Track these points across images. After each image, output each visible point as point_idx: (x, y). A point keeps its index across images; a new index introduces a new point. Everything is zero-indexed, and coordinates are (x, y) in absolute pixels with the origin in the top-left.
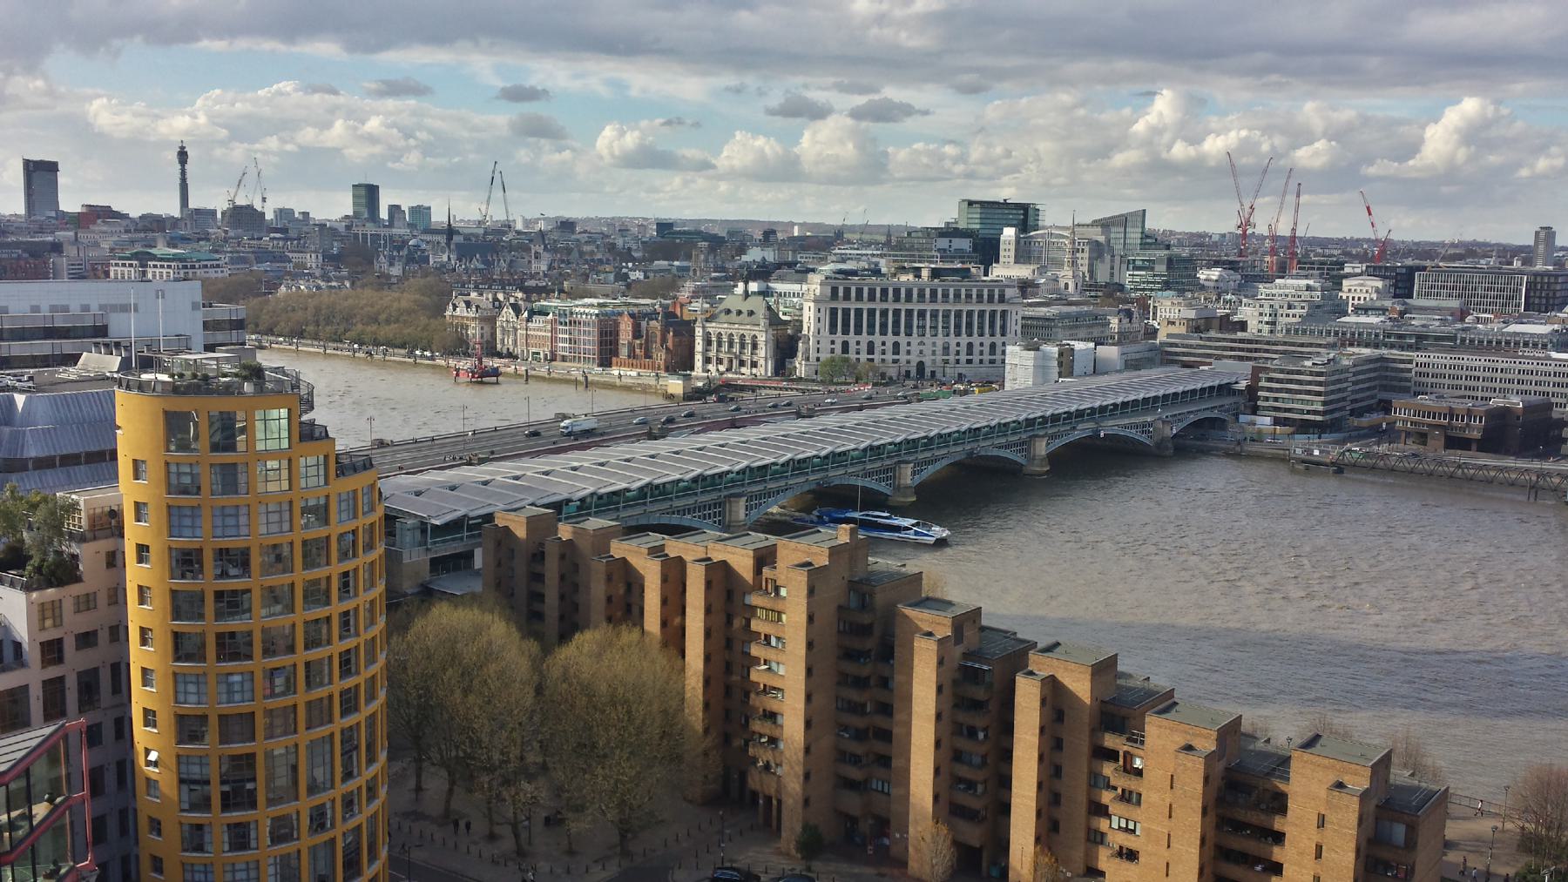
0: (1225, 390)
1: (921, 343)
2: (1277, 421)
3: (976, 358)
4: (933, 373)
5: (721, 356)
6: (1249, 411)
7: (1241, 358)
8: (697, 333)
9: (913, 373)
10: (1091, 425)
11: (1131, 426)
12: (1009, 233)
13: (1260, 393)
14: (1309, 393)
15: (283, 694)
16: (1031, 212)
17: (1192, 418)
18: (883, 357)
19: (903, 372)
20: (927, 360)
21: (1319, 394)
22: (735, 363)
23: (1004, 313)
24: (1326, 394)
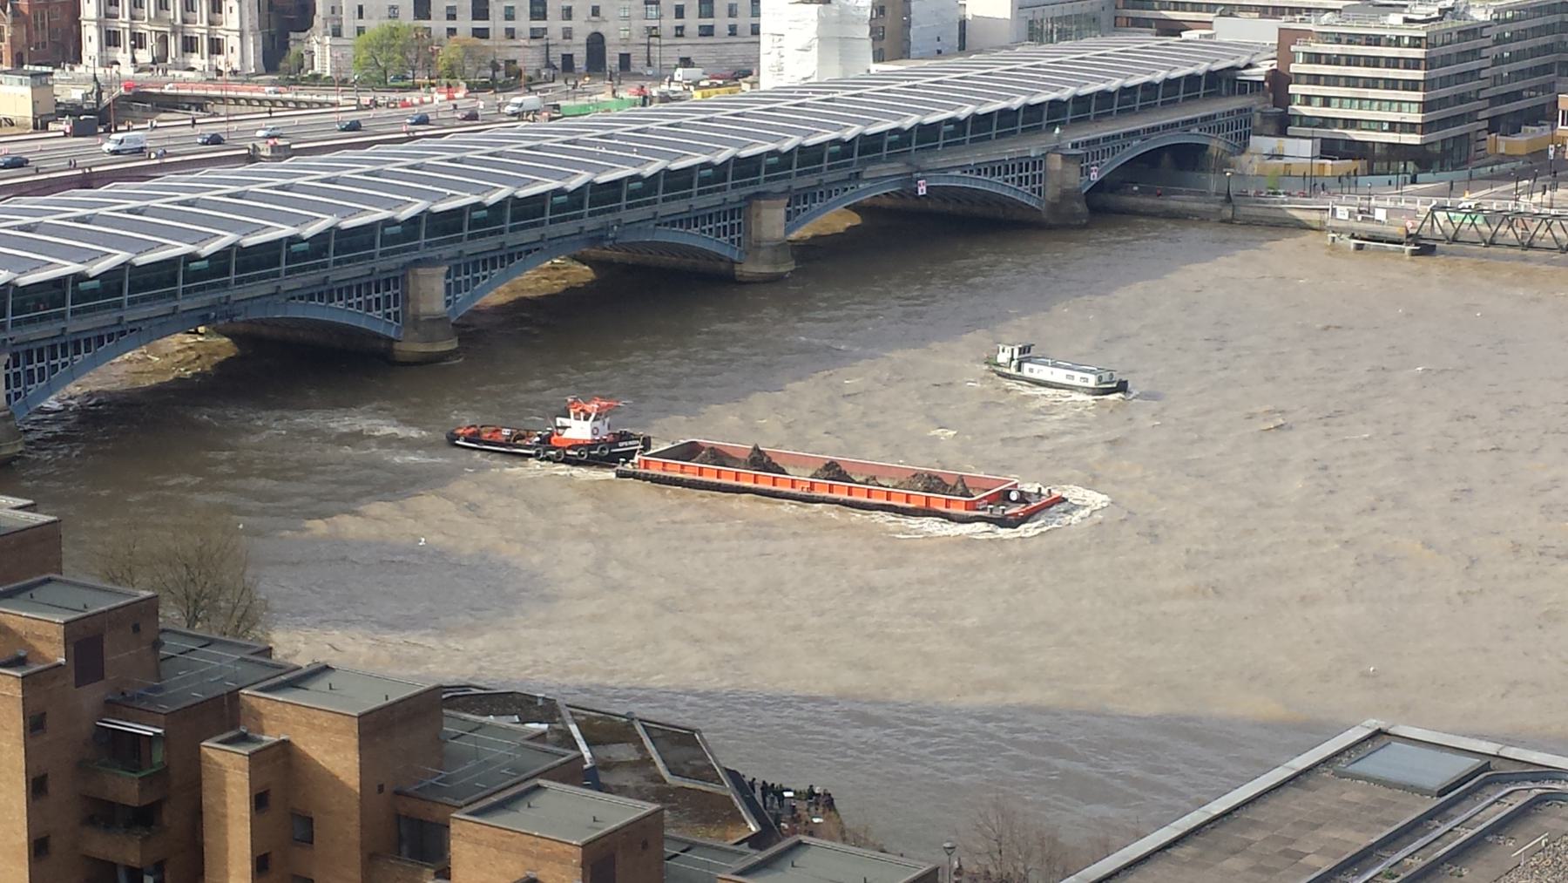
0: (1222, 82)
4: (625, 60)
5: (143, 27)
6: (1271, 127)
10: (897, 167)
11: (993, 169)
13: (1293, 89)
14: (1392, 84)
17: (1138, 147)
18: (510, 24)
19: (556, 59)
21: (1412, 85)
22: (173, 45)
24: (1428, 84)
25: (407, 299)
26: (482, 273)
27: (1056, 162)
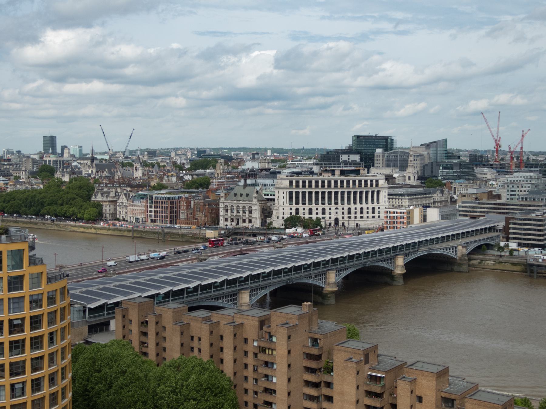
1: (337, 208)
2: (520, 245)
3: (365, 215)
4: (343, 224)
7: (500, 213)
8: (220, 206)
9: (333, 223)
12: (379, 151)
15: (20, 396)
16: (389, 140)
17: (477, 244)
19: (328, 224)
20: (340, 217)
22: (241, 221)
23: (378, 192)
25: (327, 278)
26: (341, 272)
27: (460, 248)
